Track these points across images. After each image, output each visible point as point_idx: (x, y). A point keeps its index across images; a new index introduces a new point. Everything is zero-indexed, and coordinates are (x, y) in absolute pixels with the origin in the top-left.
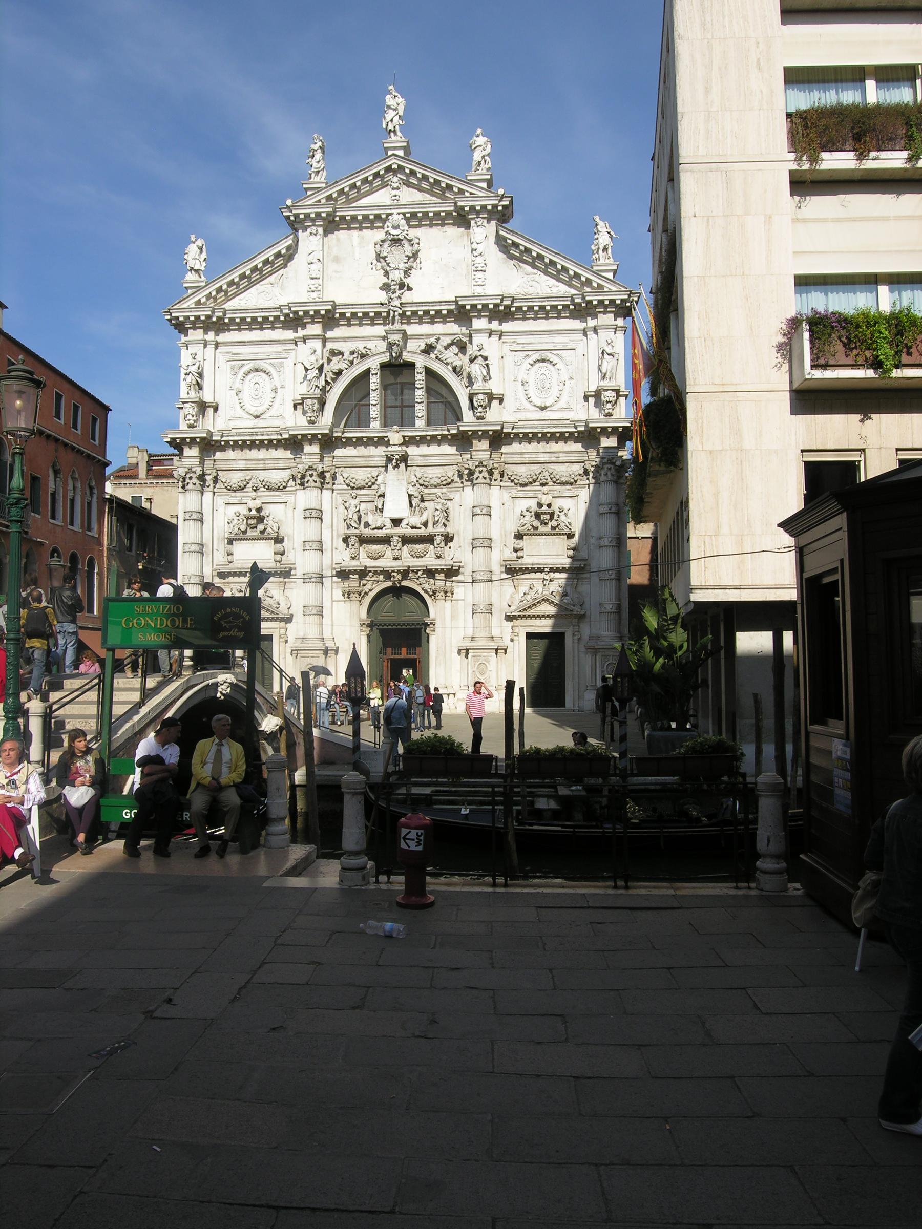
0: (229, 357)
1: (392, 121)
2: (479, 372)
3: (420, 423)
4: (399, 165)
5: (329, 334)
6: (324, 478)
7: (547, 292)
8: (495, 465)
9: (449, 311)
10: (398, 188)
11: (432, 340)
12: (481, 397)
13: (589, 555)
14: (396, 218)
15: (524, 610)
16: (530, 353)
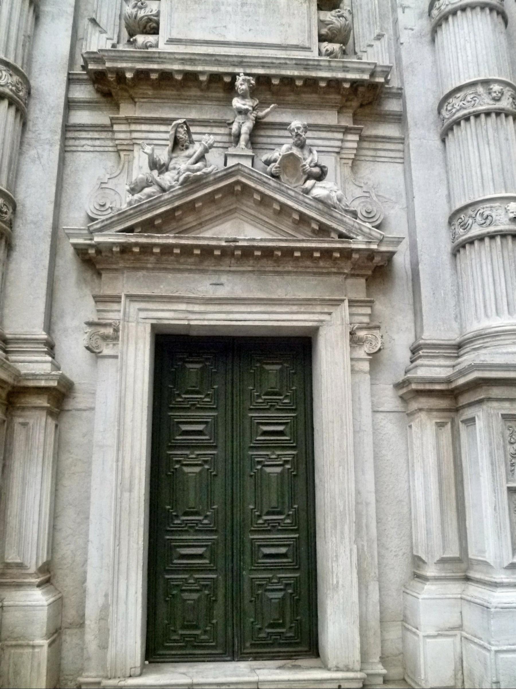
15: (149, 226)
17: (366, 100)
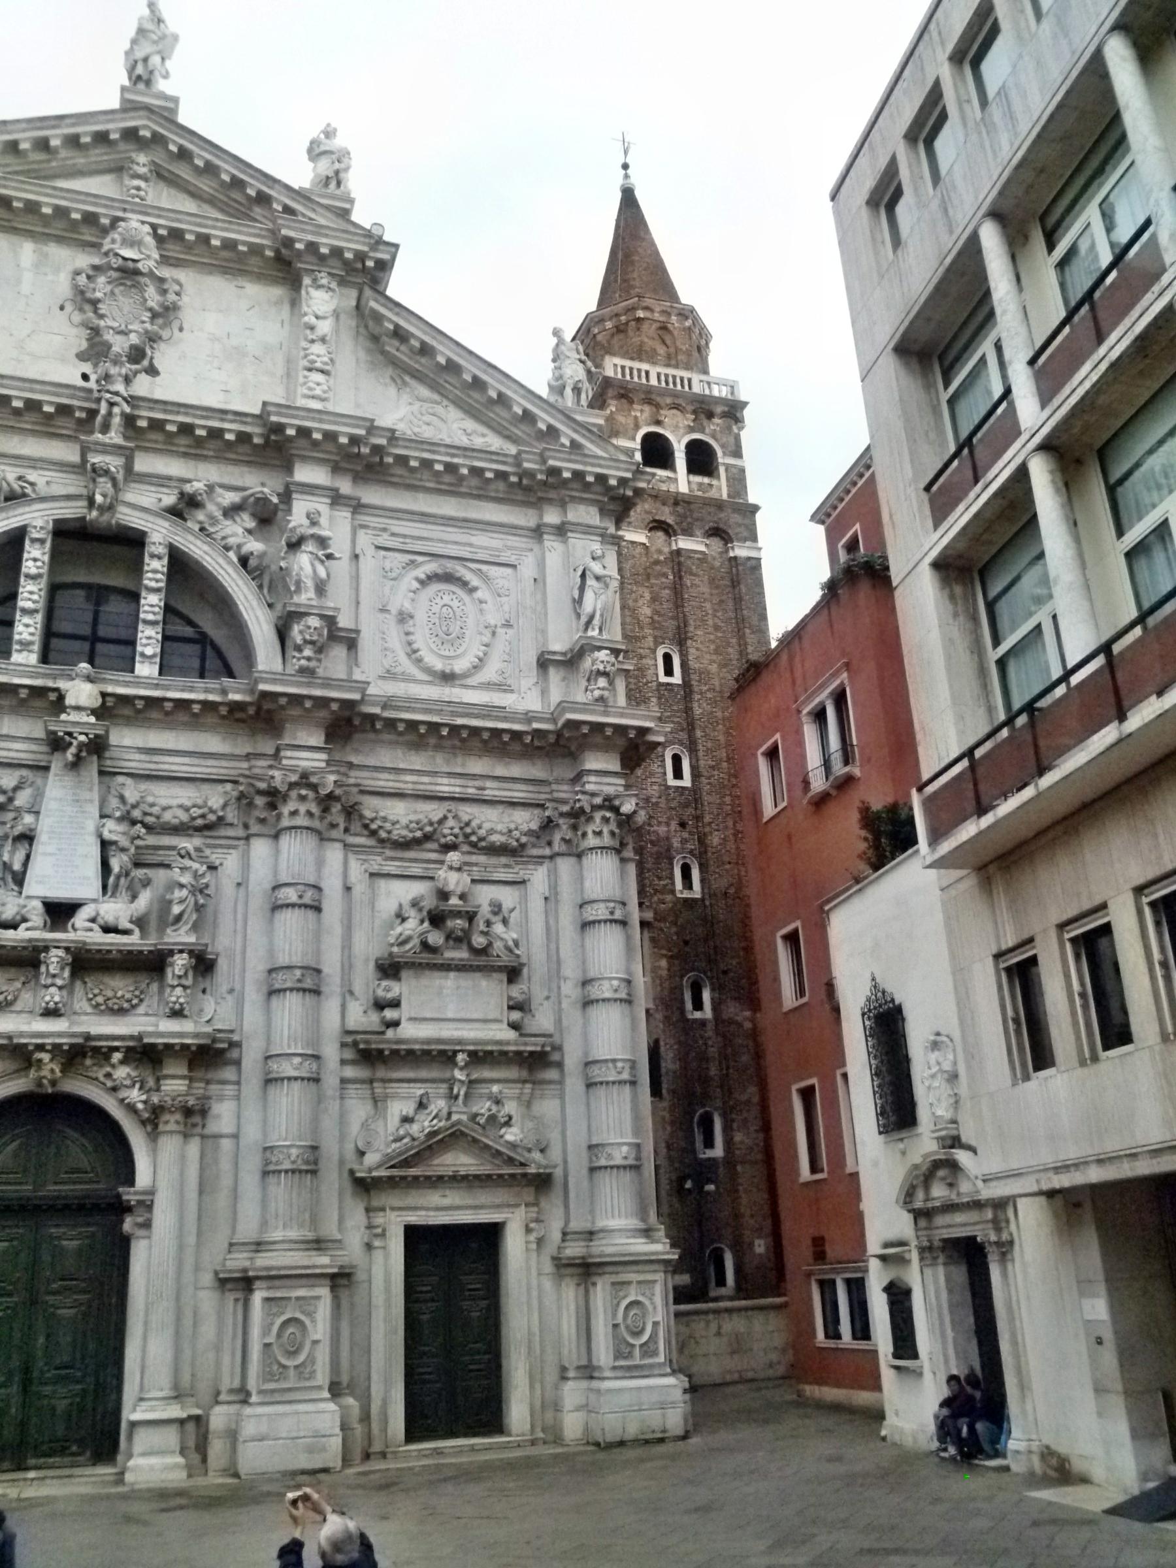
1: (145, 60)
2: (308, 569)
3: (146, 670)
7: (464, 441)
9: (244, 438)
10: (146, 180)
12: (314, 622)
13: (559, 1021)
14: (134, 224)
15: (406, 1163)
16: (420, 559)
17: (536, 1062)
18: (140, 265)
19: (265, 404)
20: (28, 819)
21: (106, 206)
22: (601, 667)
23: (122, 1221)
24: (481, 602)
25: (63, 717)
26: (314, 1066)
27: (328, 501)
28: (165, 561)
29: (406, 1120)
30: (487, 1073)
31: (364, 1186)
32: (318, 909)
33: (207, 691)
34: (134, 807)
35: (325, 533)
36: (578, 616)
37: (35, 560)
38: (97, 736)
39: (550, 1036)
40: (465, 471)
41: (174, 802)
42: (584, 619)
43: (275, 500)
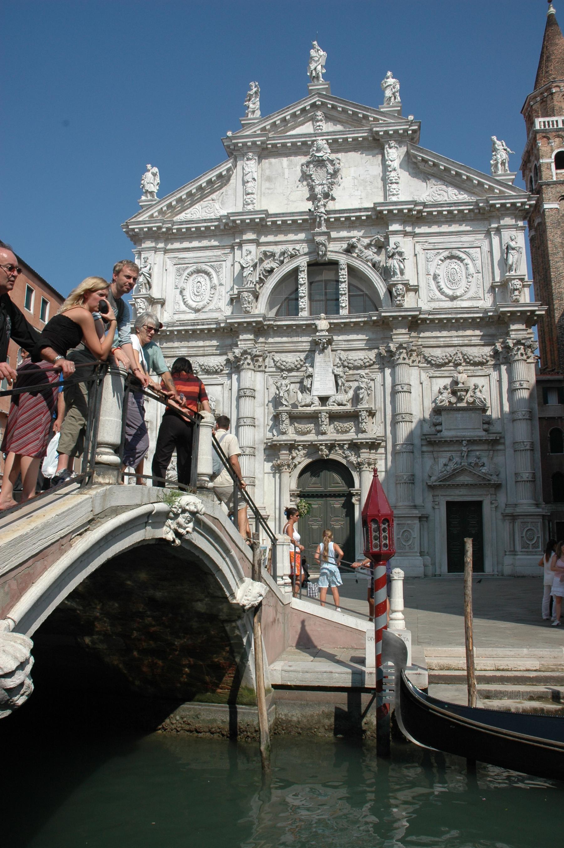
0: (175, 261)
2: (397, 266)
4: (322, 102)
5: (263, 239)
6: (257, 361)
7: (454, 199)
8: (414, 348)
10: (321, 121)
11: (354, 240)
13: (503, 427)
18: (324, 158)
19: (374, 204)
20: (310, 369)
21: (309, 137)
22: (515, 287)
23: (352, 498)
24: (467, 265)
25: (318, 334)
26: (411, 447)
27: (403, 235)
28: (346, 270)
29: (445, 465)
30: (475, 448)
31: (431, 488)
32: (411, 393)
33: (364, 317)
34: (344, 361)
35: (403, 250)
36: (506, 265)
37: (302, 278)
38: (329, 339)
39: (500, 433)
40: (456, 212)
41: (357, 358)
42: (508, 268)
43: (383, 240)
